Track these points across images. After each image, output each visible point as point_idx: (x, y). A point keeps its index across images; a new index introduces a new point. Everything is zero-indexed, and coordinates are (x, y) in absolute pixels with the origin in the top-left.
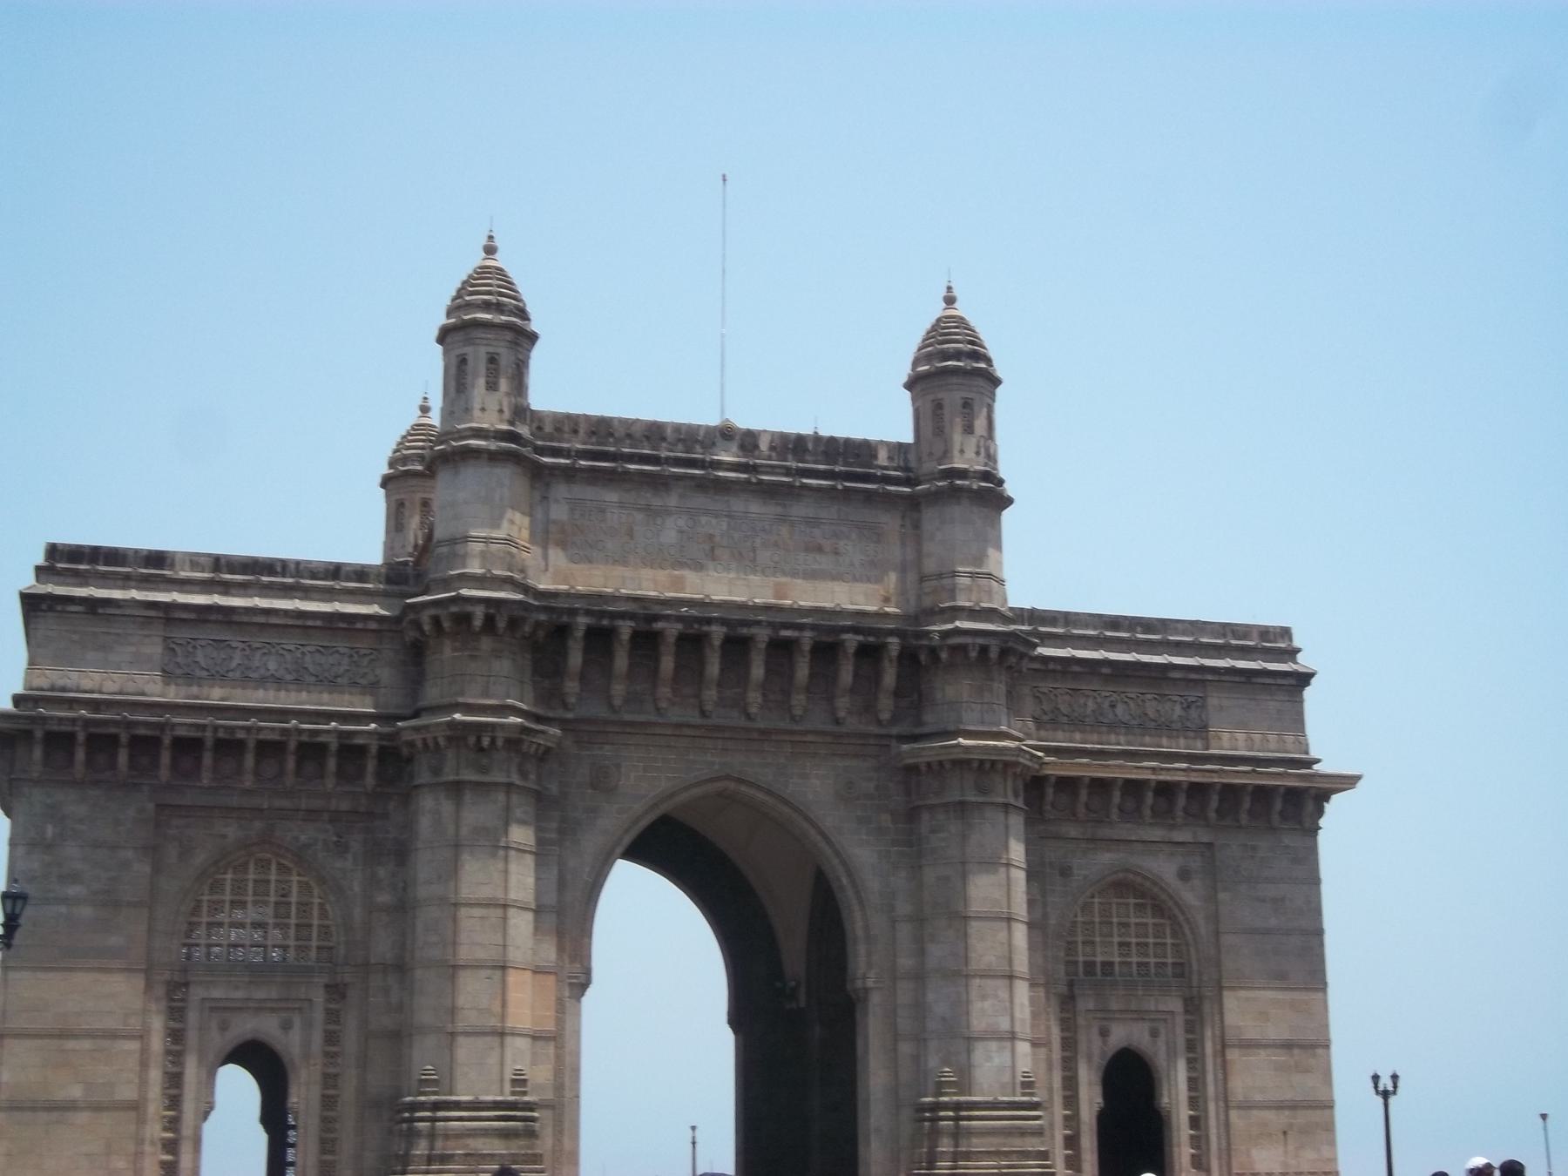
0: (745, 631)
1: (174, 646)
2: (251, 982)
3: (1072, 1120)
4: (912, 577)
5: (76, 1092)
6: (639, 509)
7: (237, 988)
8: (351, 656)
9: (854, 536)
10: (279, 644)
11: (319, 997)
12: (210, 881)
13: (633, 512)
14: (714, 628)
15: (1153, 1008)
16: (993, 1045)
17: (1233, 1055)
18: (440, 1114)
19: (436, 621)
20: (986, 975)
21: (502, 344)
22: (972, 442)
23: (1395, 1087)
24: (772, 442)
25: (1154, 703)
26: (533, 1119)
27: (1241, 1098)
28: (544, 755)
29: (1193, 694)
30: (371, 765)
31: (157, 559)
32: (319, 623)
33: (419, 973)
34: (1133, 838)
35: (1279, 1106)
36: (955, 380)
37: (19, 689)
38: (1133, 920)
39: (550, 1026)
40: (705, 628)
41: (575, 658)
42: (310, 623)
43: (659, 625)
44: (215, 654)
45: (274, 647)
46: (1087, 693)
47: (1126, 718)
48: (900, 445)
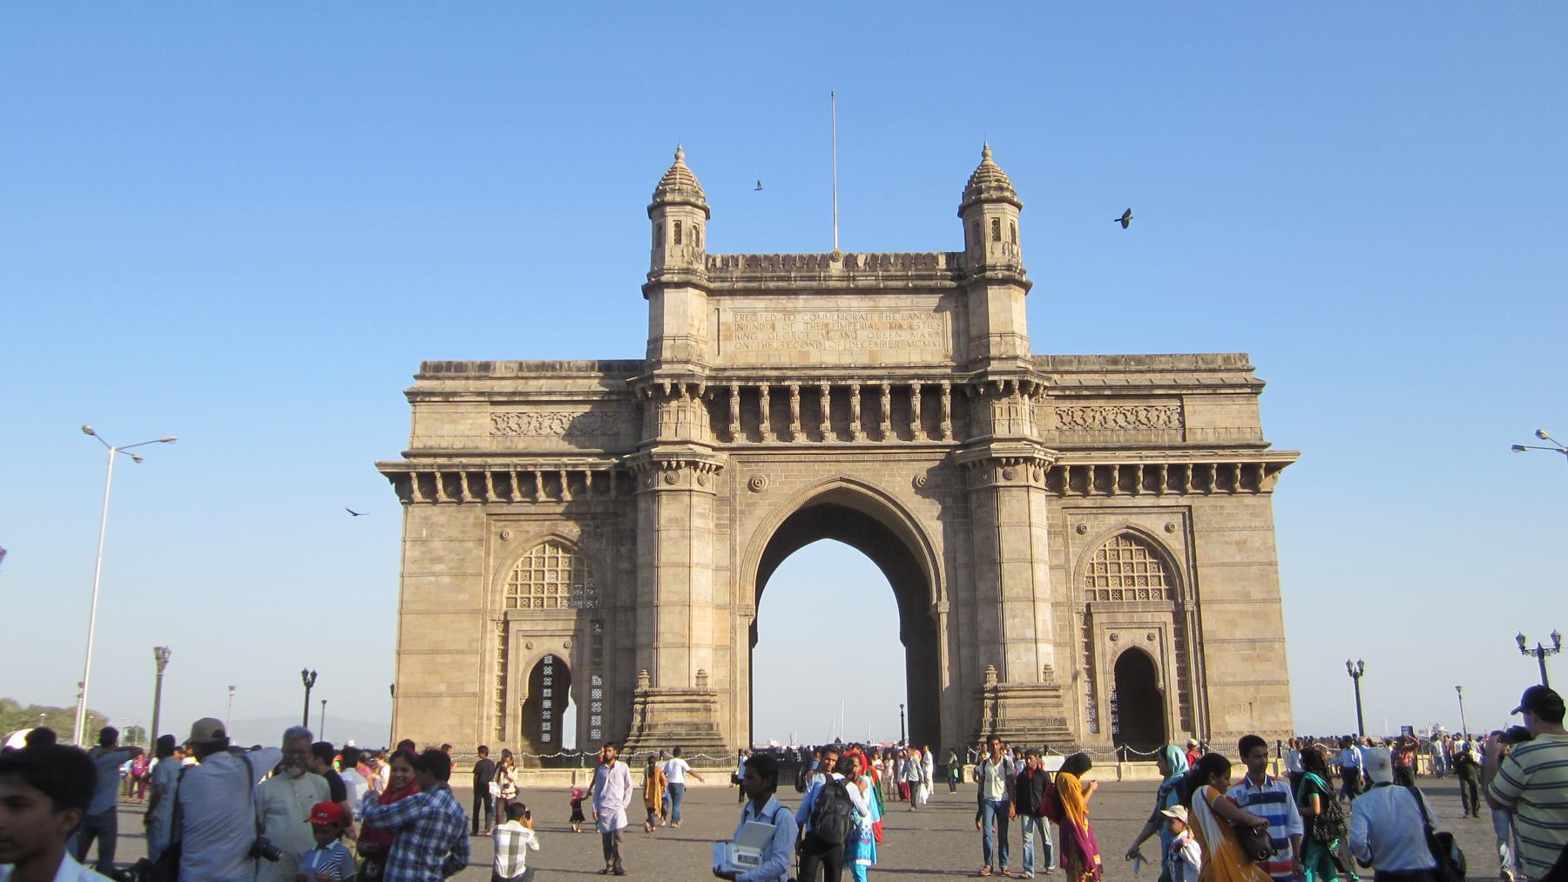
0: (843, 383)
2: (546, 620)
3: (1093, 694)
4: (963, 340)
5: (443, 688)
6: (778, 312)
7: (537, 624)
9: (923, 316)
12: (522, 559)
14: (822, 383)
15: (1150, 621)
18: (649, 699)
20: (1017, 599)
22: (999, 245)
23: (1362, 671)
25: (1145, 413)
27: (1216, 679)
28: (718, 468)
30: (613, 483)
31: (486, 367)
32: (581, 398)
33: (639, 611)
34: (1131, 505)
35: (1247, 684)
36: (986, 206)
37: (406, 449)
40: (817, 383)
41: (735, 408)
42: (576, 398)
43: (787, 383)
46: (1095, 409)
48: (953, 254)
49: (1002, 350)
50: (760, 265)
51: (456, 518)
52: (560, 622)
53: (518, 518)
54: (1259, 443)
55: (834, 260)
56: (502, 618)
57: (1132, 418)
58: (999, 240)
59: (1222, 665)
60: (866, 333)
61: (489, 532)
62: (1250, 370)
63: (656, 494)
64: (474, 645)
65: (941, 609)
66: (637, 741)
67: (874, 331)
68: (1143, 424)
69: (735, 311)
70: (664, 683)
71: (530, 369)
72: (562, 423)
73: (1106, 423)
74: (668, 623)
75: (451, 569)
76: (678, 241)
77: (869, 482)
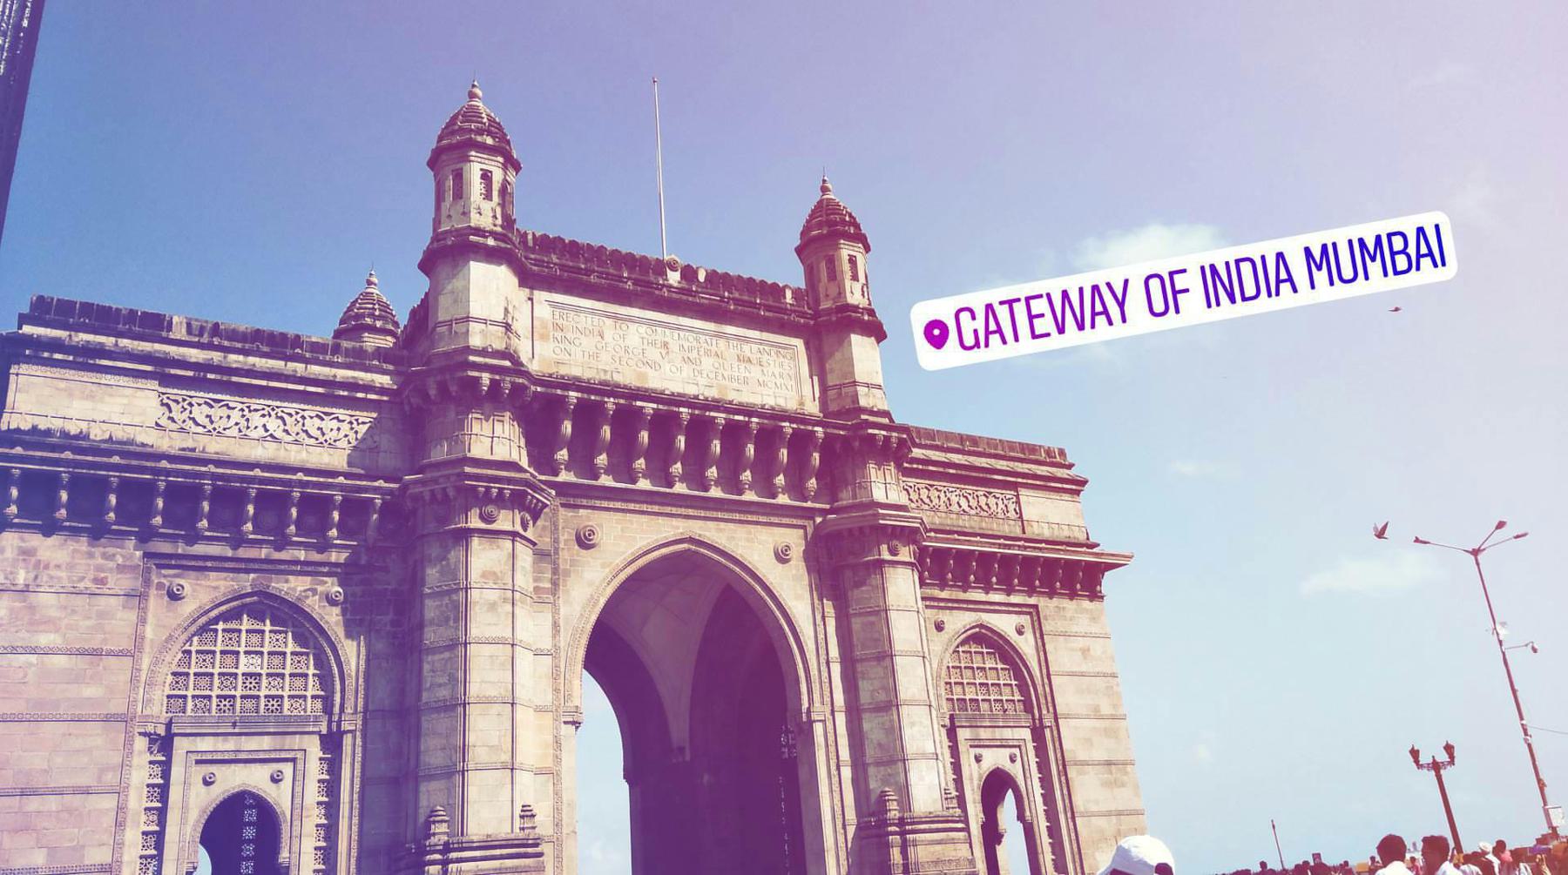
1: (170, 402)
6: (608, 317)
10: (277, 407)
14: (682, 409)
16: (923, 764)
17: (1072, 772)
18: (454, 855)
19: (443, 388)
21: (493, 163)
26: (540, 855)
27: (1082, 809)
29: (1010, 493)
31: (154, 326)
32: (320, 390)
35: (1108, 814)
38: (988, 666)
39: (549, 763)
43: (639, 403)
45: (273, 409)
47: (967, 509)
51: (91, 555)
52: (266, 738)
53: (201, 565)
55: (673, 269)
56: (161, 731)
57: (973, 503)
58: (858, 281)
59: (1088, 791)
61: (147, 582)
62: (1070, 466)
63: (465, 535)
65: (814, 717)
68: (983, 510)
71: (233, 335)
72: (285, 425)
76: (488, 196)
77: (725, 547)
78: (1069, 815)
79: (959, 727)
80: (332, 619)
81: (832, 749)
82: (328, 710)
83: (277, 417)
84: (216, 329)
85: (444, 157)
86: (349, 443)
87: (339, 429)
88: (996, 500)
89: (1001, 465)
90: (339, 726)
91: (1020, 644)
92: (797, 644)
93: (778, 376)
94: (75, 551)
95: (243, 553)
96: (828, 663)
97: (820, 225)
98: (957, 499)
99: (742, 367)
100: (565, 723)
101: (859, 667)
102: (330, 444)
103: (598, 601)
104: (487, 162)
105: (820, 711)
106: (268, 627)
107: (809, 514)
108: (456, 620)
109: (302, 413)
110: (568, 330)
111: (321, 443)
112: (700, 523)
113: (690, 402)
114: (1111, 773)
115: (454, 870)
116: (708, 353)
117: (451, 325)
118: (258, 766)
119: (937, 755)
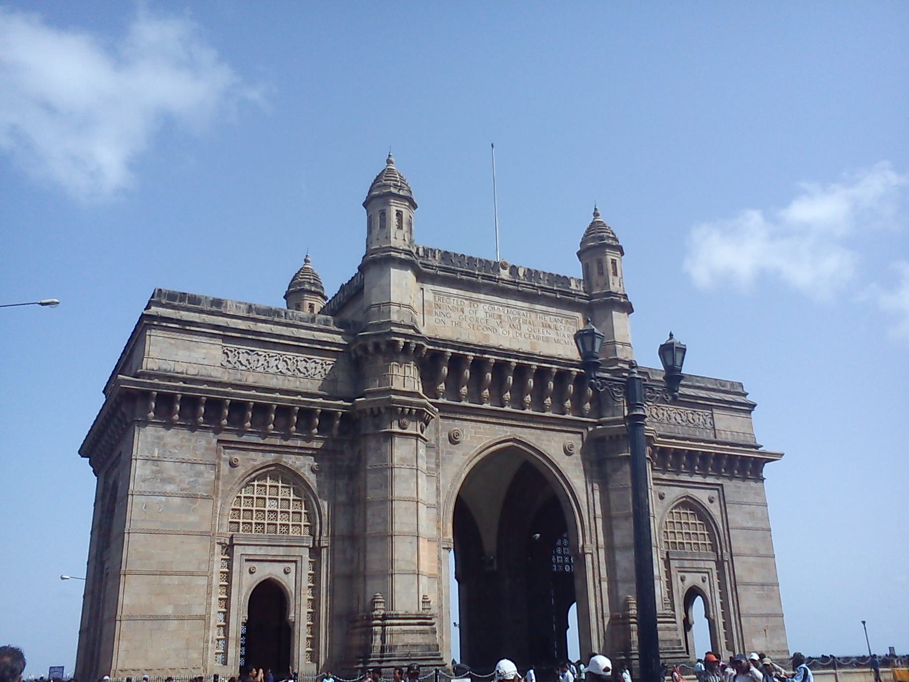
0: (526, 362)
5: (169, 610)
7: (260, 549)
8: (322, 364)
10: (284, 355)
11: (306, 553)
13: (464, 301)
14: (511, 360)
17: (740, 589)
18: (388, 621)
19: (377, 346)
21: (403, 206)
22: (617, 279)
24: (524, 272)
25: (691, 415)
35: (762, 616)
39: (436, 572)
43: (487, 356)
44: (249, 357)
45: (281, 356)
47: (680, 422)
49: (624, 355)
50: (452, 261)
51: (189, 440)
54: (754, 444)
55: (504, 268)
57: (684, 418)
59: (749, 600)
60: (527, 326)
64: (204, 565)
65: (587, 551)
66: (380, 662)
67: (532, 327)
69: (434, 292)
70: (400, 608)
71: (258, 311)
72: (287, 365)
73: (670, 419)
74: (402, 550)
75: (182, 490)
76: (400, 227)
78: (737, 615)
79: (672, 559)
80: (312, 479)
81: (596, 571)
82: (312, 534)
83: (283, 361)
84: (250, 308)
85: (374, 202)
86: (322, 376)
87: (316, 368)
88: (698, 416)
89: (702, 394)
90: (319, 543)
91: (711, 509)
92: (576, 506)
93: (566, 336)
94: (182, 438)
95: (268, 441)
96: (595, 518)
97: (593, 239)
98: (674, 415)
99: (545, 331)
100: (444, 548)
101: (614, 522)
102: (311, 377)
103: (461, 475)
104: (399, 205)
105: (589, 548)
106: (280, 485)
107: (585, 425)
108: (386, 487)
109: (296, 358)
110: (444, 308)
111: (307, 376)
112: (519, 429)
113: (516, 354)
114: (763, 590)
115: (389, 630)
116: (525, 322)
117: (380, 306)
118: (277, 564)
119: (660, 577)
